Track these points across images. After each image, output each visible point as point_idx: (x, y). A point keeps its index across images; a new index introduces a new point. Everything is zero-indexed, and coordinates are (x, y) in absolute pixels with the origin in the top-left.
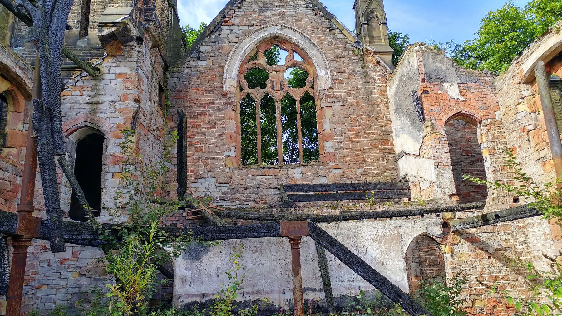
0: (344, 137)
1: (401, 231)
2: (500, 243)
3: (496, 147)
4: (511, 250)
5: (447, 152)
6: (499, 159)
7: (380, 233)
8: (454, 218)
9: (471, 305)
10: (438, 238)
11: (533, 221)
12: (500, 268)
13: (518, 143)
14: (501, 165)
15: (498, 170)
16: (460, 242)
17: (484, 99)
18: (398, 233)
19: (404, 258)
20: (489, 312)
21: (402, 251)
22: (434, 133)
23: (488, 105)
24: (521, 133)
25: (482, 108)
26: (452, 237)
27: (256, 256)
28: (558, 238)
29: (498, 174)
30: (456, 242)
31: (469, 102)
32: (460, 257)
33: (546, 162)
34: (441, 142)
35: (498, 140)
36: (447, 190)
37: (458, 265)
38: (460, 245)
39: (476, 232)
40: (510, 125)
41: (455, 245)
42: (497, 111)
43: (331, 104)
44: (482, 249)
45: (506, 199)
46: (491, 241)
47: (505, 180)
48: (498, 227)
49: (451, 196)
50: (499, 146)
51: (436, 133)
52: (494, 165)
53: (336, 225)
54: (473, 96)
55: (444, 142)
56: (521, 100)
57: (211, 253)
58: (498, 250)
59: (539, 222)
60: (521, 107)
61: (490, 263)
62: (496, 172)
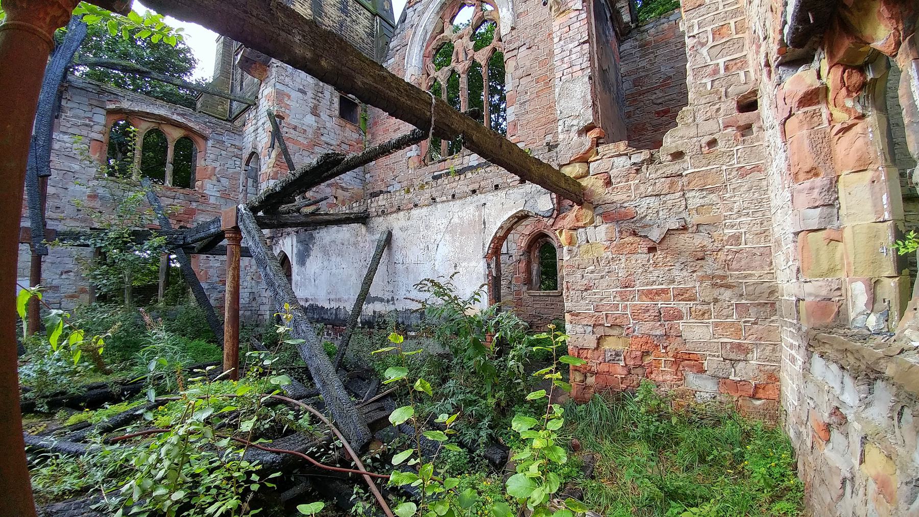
0: (529, 94)
1: (486, 211)
2: (684, 215)
4: (714, 229)
5: (584, 43)
6: (709, 15)
7: (456, 220)
8: (588, 172)
9: (593, 345)
10: (548, 217)
12: (675, 272)
14: (712, 27)
15: (705, 40)
16: (592, 222)
18: (480, 215)
19: (485, 257)
20: (631, 363)
21: (484, 244)
22: (561, 13)
26: (575, 214)
27: (339, 259)
28: (802, 176)
29: (704, 51)
30: (581, 224)
32: (587, 252)
36: (575, 122)
37: (578, 268)
38: (590, 229)
39: (628, 198)
41: (580, 230)
43: (515, 52)
44: (635, 234)
45: (717, 106)
46: (661, 213)
47: (721, 62)
48: (685, 179)
49: (588, 129)
51: (564, 11)
52: (696, 32)
53: (407, 214)
57: (311, 258)
58: (672, 232)
61: (651, 262)
62: (699, 47)
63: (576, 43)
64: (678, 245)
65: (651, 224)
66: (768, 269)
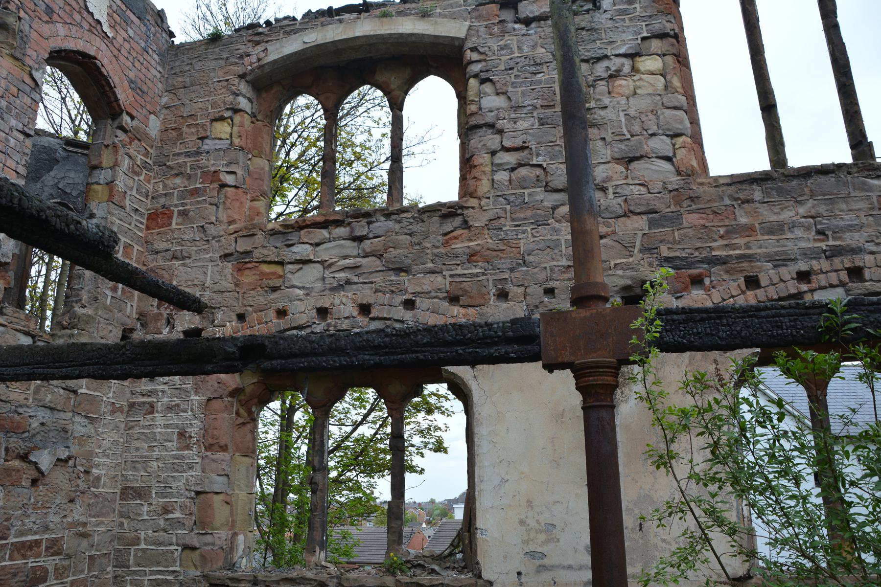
3: (129, 193)
11: (155, 400)
13: (183, 204)
17: (143, 70)
23: (145, 88)
24: (200, 183)
25: (133, 86)
31: (116, 52)
33: (249, 265)
34: (23, 97)
35: (136, 178)
40: (176, 158)
42: (154, 113)
50: (134, 193)
54: (127, 45)
55: (29, 100)
56: (227, 114)
59: (173, 403)
60: (223, 129)
63: (20, 127)
64: (57, 481)
65: (41, 446)
66: (112, 516)
